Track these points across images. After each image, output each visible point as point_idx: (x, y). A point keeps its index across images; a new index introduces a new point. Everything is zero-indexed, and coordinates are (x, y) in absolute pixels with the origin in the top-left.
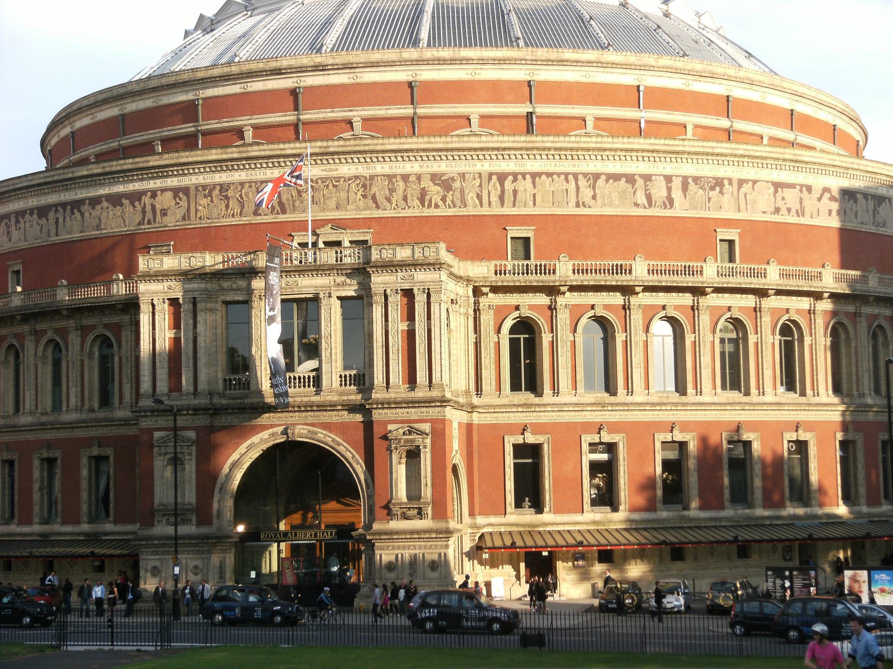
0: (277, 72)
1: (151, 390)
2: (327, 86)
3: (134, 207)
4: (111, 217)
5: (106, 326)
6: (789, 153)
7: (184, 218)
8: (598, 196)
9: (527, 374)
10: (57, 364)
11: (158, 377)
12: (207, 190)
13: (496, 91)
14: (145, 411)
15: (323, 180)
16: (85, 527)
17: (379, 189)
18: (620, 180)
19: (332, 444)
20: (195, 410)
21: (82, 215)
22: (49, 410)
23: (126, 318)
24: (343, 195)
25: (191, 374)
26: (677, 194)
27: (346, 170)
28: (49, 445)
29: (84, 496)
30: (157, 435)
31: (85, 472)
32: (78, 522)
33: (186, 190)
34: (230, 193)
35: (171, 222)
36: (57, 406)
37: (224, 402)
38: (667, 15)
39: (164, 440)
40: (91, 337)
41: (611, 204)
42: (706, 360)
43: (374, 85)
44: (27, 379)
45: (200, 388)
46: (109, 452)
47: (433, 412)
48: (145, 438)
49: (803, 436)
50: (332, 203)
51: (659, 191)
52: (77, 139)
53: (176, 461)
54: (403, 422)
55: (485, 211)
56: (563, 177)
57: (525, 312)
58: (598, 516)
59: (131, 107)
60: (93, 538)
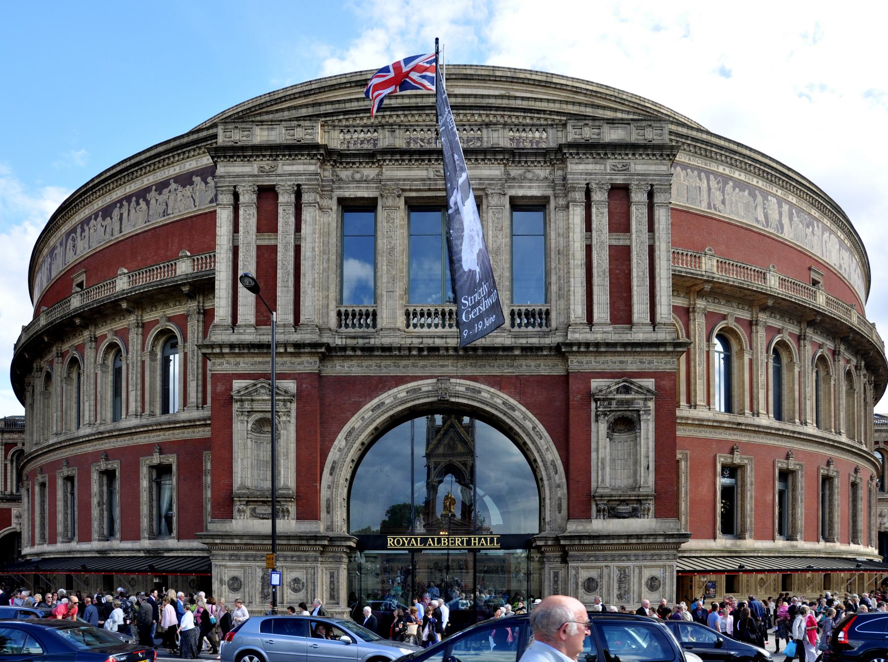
1: (229, 321)
3: (206, 183)
4: (179, 199)
8: (727, 202)
14: (221, 346)
18: (742, 190)
19: (502, 407)
21: (148, 203)
30: (237, 384)
37: (339, 342)
48: (220, 388)
56: (696, 173)
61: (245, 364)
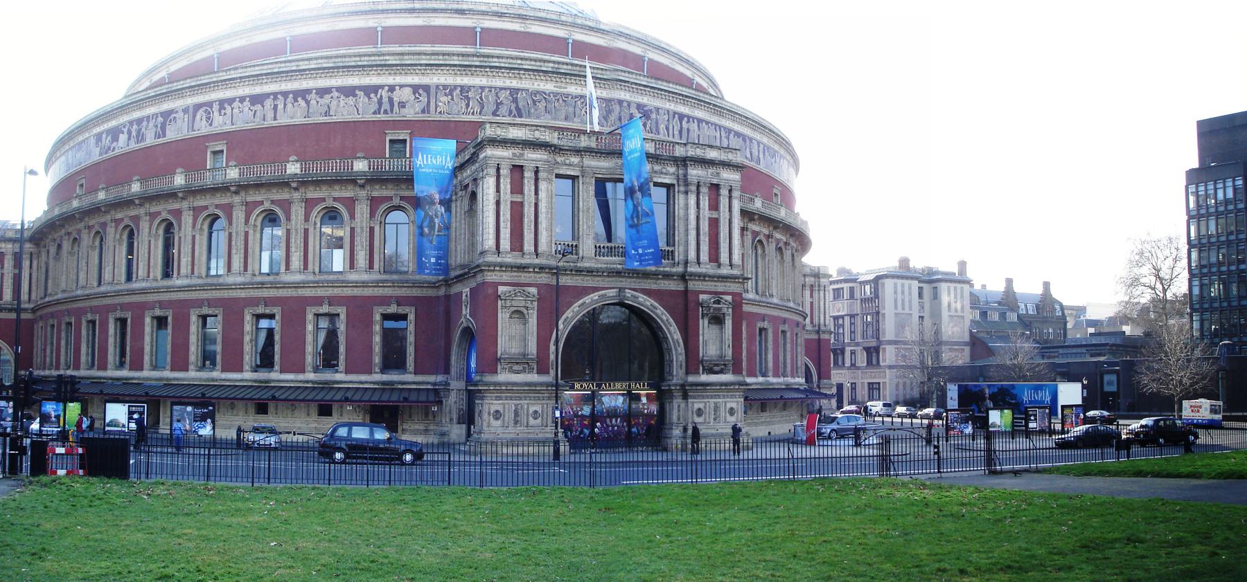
2: (501, 30)
5: (335, 199)
7: (423, 111)
11: (502, 236)
12: (449, 90)
15: (555, 94)
20: (541, 268)
22: (257, 273)
24: (571, 110)
25: (532, 236)
30: (501, 289)
34: (470, 95)
40: (319, 208)
43: (540, 35)
45: (540, 250)
47: (735, 287)
48: (490, 291)
53: (519, 314)
54: (710, 293)
61: (506, 277)
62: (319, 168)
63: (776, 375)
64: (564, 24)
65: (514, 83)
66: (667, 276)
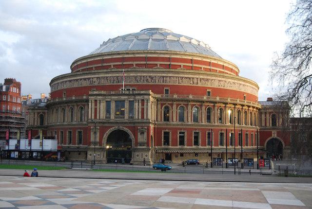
0: (119, 54)
6: (222, 74)
9: (166, 119)
10: (72, 112)
12: (103, 78)
13: (163, 59)
16: (77, 146)
17: (138, 79)
23: (86, 103)
26: (199, 82)
27: (132, 75)
28: (70, 128)
29: (77, 139)
30: (92, 127)
31: (77, 135)
32: (75, 144)
33: (99, 78)
35: (96, 84)
36: (72, 121)
38: (199, 45)
39: (93, 128)
41: (185, 83)
42: (203, 116)
44: (66, 115)
46: (82, 131)
49: (223, 132)
50: (129, 81)
51: (195, 81)
52: (78, 66)
53: (95, 133)
55: (160, 84)
57: (167, 105)
58: (180, 147)
59: (89, 60)
60: (78, 148)
61: (93, 125)
62: (77, 98)
63: (204, 144)
64: (144, 53)
65: (118, 75)
66: (130, 123)
